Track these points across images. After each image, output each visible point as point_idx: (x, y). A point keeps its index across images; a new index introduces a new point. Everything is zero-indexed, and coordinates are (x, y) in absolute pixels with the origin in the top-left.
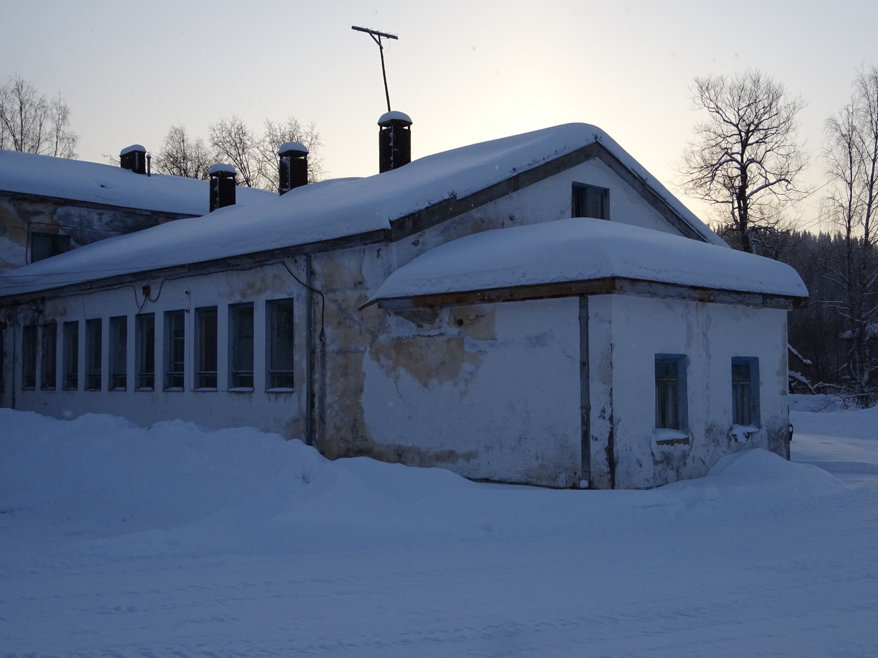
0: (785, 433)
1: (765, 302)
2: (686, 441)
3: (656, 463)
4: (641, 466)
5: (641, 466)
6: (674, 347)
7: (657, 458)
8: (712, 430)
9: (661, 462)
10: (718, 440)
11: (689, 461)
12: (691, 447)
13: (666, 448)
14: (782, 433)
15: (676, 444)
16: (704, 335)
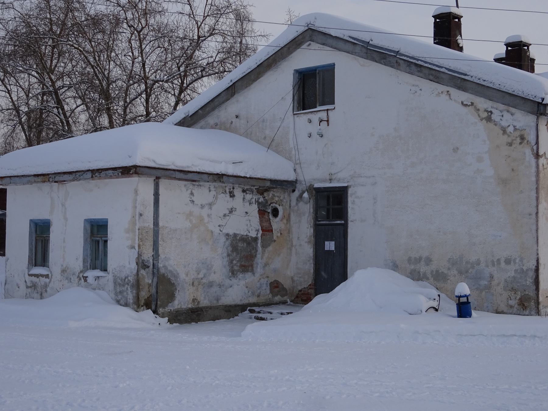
0: (131, 280)
1: (94, 176)
2: (47, 276)
3: (27, 287)
4: (19, 287)
5: (19, 287)
6: (41, 215)
7: (28, 285)
8: (66, 271)
9: (30, 287)
10: (71, 279)
11: (48, 289)
12: (50, 280)
13: (34, 279)
14: (128, 280)
15: (40, 277)
16: (63, 205)
